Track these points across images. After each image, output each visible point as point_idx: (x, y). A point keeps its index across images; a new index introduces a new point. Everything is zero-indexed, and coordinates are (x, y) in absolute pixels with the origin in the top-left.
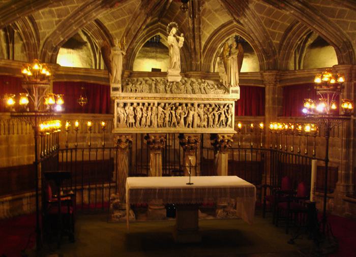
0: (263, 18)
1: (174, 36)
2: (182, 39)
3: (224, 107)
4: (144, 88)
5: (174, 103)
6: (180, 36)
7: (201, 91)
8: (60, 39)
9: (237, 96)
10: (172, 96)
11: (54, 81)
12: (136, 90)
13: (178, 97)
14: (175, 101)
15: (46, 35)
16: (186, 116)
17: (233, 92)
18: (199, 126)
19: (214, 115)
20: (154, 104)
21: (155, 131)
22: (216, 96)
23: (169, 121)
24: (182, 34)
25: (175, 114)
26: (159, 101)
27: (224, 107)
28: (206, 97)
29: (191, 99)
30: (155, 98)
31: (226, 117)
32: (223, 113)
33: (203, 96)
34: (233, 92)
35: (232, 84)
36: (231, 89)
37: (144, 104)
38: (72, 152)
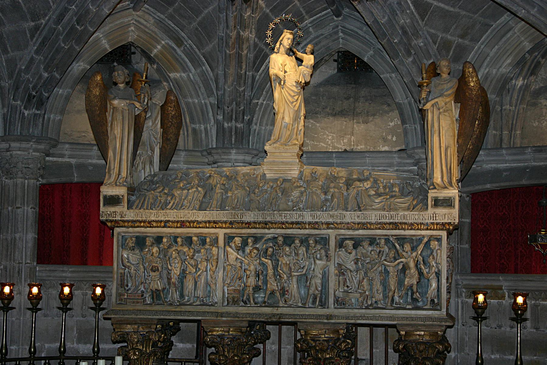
1: (290, 52)
2: (309, 59)
3: (414, 249)
8: (41, 76)
9: (451, 215)
10: (261, 219)
11: (42, 181)
12: (166, 204)
13: (279, 219)
14: (272, 231)
16: (304, 272)
17: (437, 203)
18: (340, 303)
19: (387, 272)
21: (217, 314)
22: (387, 217)
23: (257, 289)
25: (275, 268)
26: (228, 231)
27: (414, 249)
28: (357, 220)
29: (314, 225)
30: (215, 222)
31: (421, 273)
32: (412, 264)
33: (350, 217)
34: (437, 203)
35: (437, 178)
36: (432, 194)
37: (188, 240)
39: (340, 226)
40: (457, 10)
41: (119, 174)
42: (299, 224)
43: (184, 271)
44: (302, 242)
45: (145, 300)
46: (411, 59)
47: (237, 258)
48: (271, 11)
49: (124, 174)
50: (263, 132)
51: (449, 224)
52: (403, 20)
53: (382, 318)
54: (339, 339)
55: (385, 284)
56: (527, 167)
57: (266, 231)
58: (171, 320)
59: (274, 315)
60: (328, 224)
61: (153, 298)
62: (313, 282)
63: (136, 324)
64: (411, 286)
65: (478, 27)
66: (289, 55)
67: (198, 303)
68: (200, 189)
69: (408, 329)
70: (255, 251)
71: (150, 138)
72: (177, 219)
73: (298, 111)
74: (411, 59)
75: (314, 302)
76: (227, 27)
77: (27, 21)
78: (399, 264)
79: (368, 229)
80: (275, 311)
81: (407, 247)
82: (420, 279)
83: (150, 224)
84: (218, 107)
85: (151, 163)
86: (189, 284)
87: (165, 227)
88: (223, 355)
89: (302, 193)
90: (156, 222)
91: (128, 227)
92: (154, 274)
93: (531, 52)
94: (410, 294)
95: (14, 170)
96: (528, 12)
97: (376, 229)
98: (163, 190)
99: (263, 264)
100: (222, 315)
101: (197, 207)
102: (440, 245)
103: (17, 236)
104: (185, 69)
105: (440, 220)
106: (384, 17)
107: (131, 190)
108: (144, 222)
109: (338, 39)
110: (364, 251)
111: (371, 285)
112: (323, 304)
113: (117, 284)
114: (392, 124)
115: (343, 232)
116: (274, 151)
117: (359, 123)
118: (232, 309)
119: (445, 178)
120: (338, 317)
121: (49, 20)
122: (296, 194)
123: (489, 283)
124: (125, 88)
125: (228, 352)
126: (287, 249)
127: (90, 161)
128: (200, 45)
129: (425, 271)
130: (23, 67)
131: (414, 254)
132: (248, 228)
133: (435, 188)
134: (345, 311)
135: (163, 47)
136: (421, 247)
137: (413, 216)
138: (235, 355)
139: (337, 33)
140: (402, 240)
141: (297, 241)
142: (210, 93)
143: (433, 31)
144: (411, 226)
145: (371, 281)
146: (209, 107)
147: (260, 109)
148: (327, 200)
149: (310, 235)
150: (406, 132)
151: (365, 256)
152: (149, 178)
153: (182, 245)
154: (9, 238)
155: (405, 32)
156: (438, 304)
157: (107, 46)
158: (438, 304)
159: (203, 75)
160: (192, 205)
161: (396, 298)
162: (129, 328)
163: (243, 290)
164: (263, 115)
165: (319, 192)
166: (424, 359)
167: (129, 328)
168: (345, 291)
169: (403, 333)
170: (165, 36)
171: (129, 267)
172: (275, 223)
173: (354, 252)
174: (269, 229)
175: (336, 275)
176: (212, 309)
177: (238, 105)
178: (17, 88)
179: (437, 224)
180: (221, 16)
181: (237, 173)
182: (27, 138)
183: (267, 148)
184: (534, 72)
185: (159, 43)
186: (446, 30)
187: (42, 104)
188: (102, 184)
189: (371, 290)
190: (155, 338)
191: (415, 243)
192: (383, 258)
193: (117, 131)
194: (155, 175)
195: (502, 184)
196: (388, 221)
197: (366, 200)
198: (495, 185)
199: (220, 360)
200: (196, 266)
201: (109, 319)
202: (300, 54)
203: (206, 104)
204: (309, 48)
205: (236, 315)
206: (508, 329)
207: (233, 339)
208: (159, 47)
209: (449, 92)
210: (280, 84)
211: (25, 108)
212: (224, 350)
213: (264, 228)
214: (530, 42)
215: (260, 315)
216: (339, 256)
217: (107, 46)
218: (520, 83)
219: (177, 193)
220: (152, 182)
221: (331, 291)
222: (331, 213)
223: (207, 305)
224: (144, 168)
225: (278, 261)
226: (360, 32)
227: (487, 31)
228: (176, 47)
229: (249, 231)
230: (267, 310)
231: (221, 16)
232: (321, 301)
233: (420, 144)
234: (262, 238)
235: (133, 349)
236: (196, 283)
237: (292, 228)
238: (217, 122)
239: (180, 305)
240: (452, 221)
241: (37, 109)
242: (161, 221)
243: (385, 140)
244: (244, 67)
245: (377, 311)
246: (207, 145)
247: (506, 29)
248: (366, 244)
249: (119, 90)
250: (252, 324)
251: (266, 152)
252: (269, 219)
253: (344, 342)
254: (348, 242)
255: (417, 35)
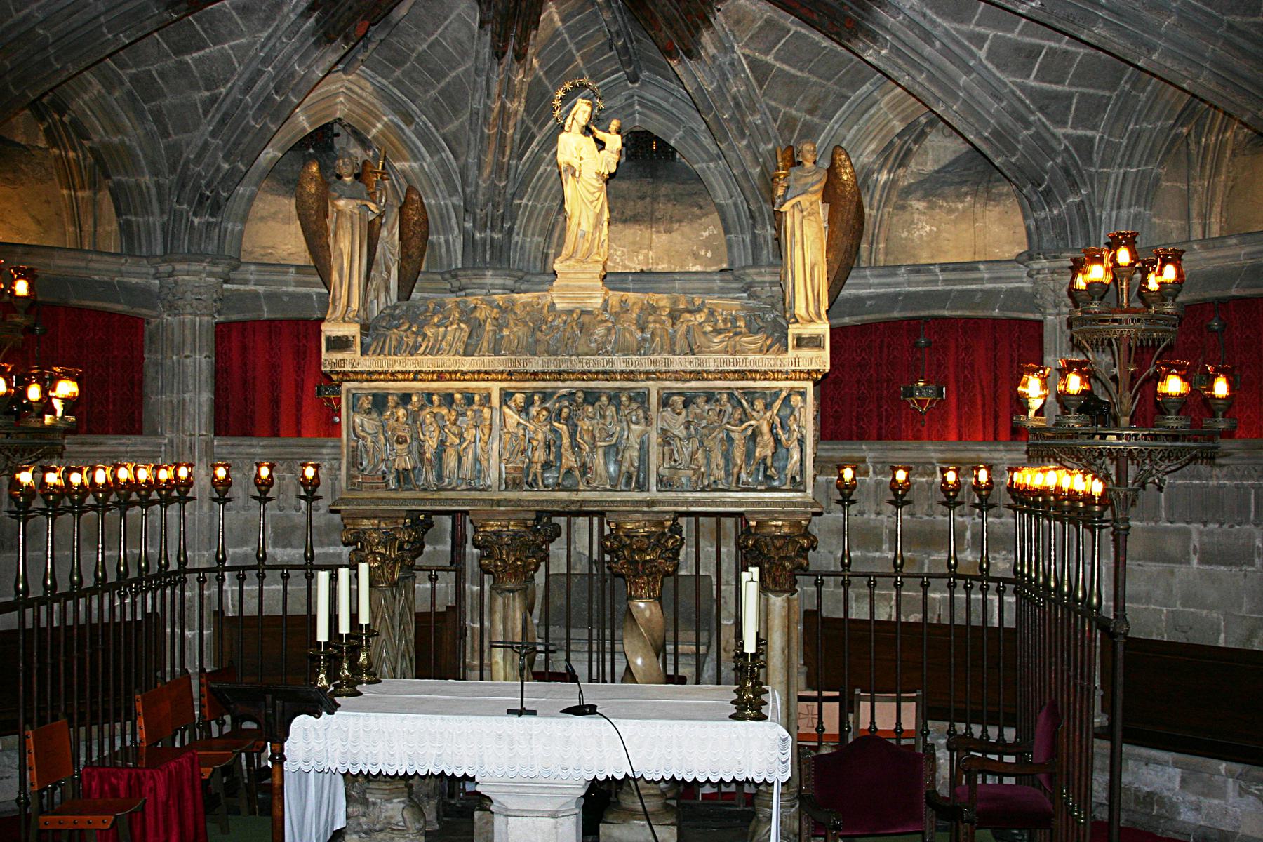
0: (979, 40)
1: (587, 131)
2: (614, 142)
3: (768, 407)
4: (449, 338)
5: (564, 391)
6: (606, 130)
7: (673, 344)
8: (219, 168)
9: (821, 360)
13: (579, 367)
14: (568, 383)
15: (181, 154)
17: (801, 342)
19: (730, 440)
20: (487, 399)
21: (492, 502)
22: (731, 363)
23: (547, 465)
24: (614, 124)
25: (572, 435)
26: (505, 385)
27: (768, 407)
28: (689, 368)
29: (629, 375)
30: (486, 372)
32: (765, 429)
33: (680, 363)
34: (801, 342)
35: (800, 310)
36: (793, 330)
37: (448, 399)
38: (242, 580)
39: (664, 376)
40: (806, 75)
41: (348, 305)
42: (608, 375)
43: (442, 443)
44: (610, 399)
45: (387, 485)
46: (744, 143)
47: (519, 423)
48: (546, 73)
49: (355, 305)
50: (527, 245)
51: (817, 371)
52: (736, 87)
53: (724, 504)
54: (664, 534)
55: (727, 457)
56: (899, 294)
57: (560, 384)
58: (422, 512)
59: (573, 502)
60: (647, 373)
61: (399, 482)
62: (627, 455)
63: (375, 518)
64: (764, 459)
65: (831, 98)
66: (585, 134)
67: (464, 487)
68: (463, 325)
69: (760, 517)
70: (545, 413)
71: (384, 255)
72: (432, 369)
73: (600, 214)
74: (744, 143)
75: (628, 483)
76: (489, 95)
77: (199, 89)
78: (746, 429)
79: (704, 379)
80: (574, 496)
81: (759, 404)
82: (776, 448)
83: (393, 376)
84: (466, 211)
85: (387, 290)
86: (451, 460)
87: (415, 379)
88: (501, 559)
89: (609, 330)
90: (403, 373)
91: (361, 381)
92: (400, 447)
93: (899, 135)
94: (762, 469)
95: (181, 303)
96: (914, 79)
97: (715, 379)
98: (410, 328)
99: (554, 431)
100: (499, 503)
101: (461, 351)
102: (804, 401)
103: (187, 396)
104: (416, 157)
105: (804, 367)
106: (712, 83)
107: (365, 329)
108: (385, 373)
109: (633, 113)
110: (698, 411)
111: (708, 459)
112: (641, 487)
113: (348, 462)
114: (706, 234)
115: (668, 384)
116: (567, 270)
117: (658, 232)
118: (512, 495)
119: (811, 309)
120: (663, 503)
121: (232, 88)
122: (600, 331)
123: (847, 454)
124: (353, 183)
125: (508, 555)
126: (590, 409)
127: (284, 289)
128: (439, 121)
129: (784, 437)
130: (192, 157)
131: (768, 414)
132: (535, 380)
133: (797, 321)
134: (673, 494)
135: (385, 125)
136: (778, 403)
137: (767, 362)
138: (518, 559)
139: (632, 105)
140: (750, 394)
141: (604, 398)
142: (452, 191)
143: (773, 103)
144: (765, 375)
145: (708, 453)
146: (452, 211)
147: (523, 214)
148: (644, 339)
149: (621, 390)
150: (730, 246)
151: (700, 417)
152: (388, 311)
153: (439, 406)
154: (175, 400)
155: (737, 105)
156: (801, 483)
157: (306, 125)
158: (801, 483)
159: (443, 164)
160: (454, 349)
161: (744, 476)
162: (366, 524)
163: (528, 467)
164: (528, 222)
165: (633, 328)
166: (782, 558)
167: (366, 524)
168: (671, 467)
169: (753, 523)
170: (388, 111)
171: (364, 438)
172: (573, 373)
173: (684, 413)
174: (563, 381)
175: (659, 445)
176: (485, 495)
177: (496, 206)
178: (183, 186)
179: (801, 372)
180: (479, 80)
181: (513, 303)
182: (198, 257)
183: (557, 266)
184: (902, 162)
185: (379, 120)
186: (790, 103)
187: (219, 208)
188: (323, 320)
189: (708, 464)
190: (403, 536)
191: (769, 398)
192: (725, 421)
193: (345, 244)
194: (395, 307)
195: (866, 317)
196: (732, 368)
197: (701, 340)
198: (855, 318)
199: (496, 566)
200: (460, 435)
201: (338, 511)
202: (600, 135)
203: (446, 206)
204: (614, 124)
205: (519, 503)
206: (873, 516)
207: (515, 536)
208: (380, 126)
209: (816, 188)
210: (573, 175)
211: (195, 214)
212: (501, 553)
213: (557, 380)
214: (902, 121)
215: (553, 502)
216: (663, 418)
217: (306, 125)
218: (884, 177)
219: (430, 331)
220: (392, 316)
221: (653, 468)
222: (652, 358)
223: (476, 490)
224: (377, 298)
225: (576, 426)
226: (664, 104)
227: (841, 106)
228: (403, 126)
229: (535, 384)
230: (563, 495)
231: (479, 80)
232: (637, 481)
233: (751, 262)
234: (553, 393)
235: (372, 552)
236: (460, 459)
237: (597, 380)
238: (464, 232)
239: (439, 490)
240: (821, 368)
241: (212, 215)
242: (409, 372)
243: (696, 256)
244: (508, 153)
245: (717, 494)
246: (450, 265)
247: (869, 102)
248: (701, 401)
249: (345, 185)
250: (540, 514)
251: (555, 273)
252: (563, 367)
253: (671, 537)
254: (675, 398)
255: (753, 109)
